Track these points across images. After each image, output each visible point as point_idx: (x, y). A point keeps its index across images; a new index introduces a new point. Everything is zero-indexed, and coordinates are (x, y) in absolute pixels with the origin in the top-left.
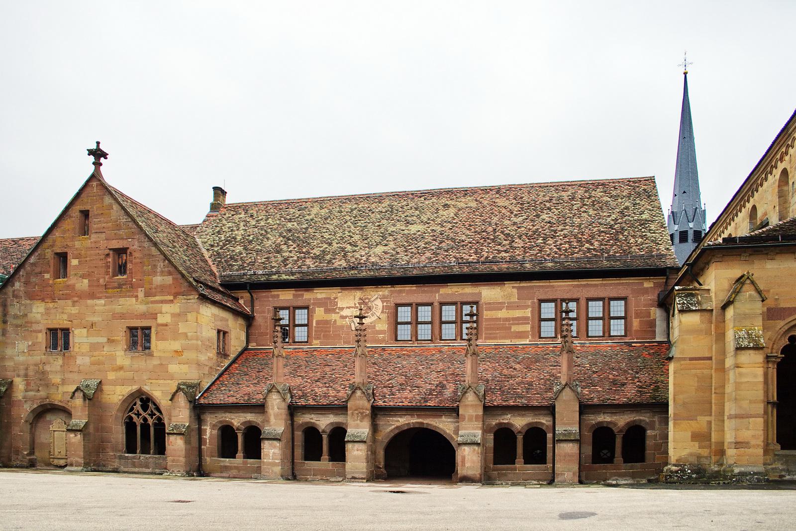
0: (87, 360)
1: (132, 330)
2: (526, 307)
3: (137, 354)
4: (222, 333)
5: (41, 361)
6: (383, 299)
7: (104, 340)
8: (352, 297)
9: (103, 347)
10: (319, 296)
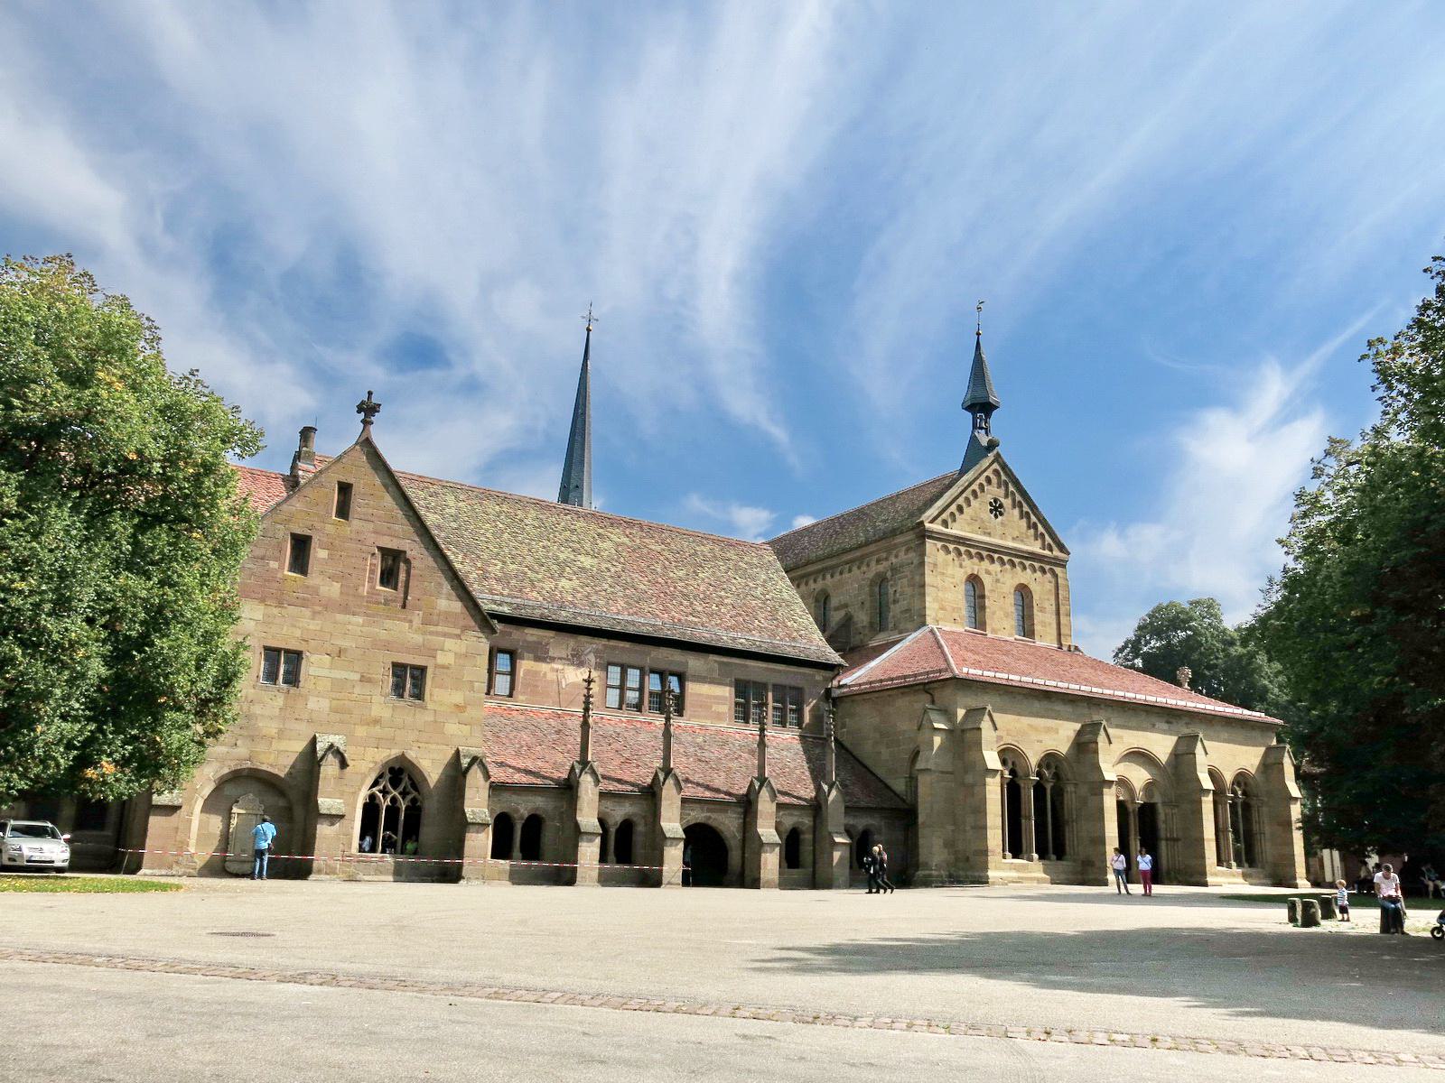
1: (399, 669)
6: (596, 652)
8: (564, 647)
9: (354, 687)
10: (530, 639)
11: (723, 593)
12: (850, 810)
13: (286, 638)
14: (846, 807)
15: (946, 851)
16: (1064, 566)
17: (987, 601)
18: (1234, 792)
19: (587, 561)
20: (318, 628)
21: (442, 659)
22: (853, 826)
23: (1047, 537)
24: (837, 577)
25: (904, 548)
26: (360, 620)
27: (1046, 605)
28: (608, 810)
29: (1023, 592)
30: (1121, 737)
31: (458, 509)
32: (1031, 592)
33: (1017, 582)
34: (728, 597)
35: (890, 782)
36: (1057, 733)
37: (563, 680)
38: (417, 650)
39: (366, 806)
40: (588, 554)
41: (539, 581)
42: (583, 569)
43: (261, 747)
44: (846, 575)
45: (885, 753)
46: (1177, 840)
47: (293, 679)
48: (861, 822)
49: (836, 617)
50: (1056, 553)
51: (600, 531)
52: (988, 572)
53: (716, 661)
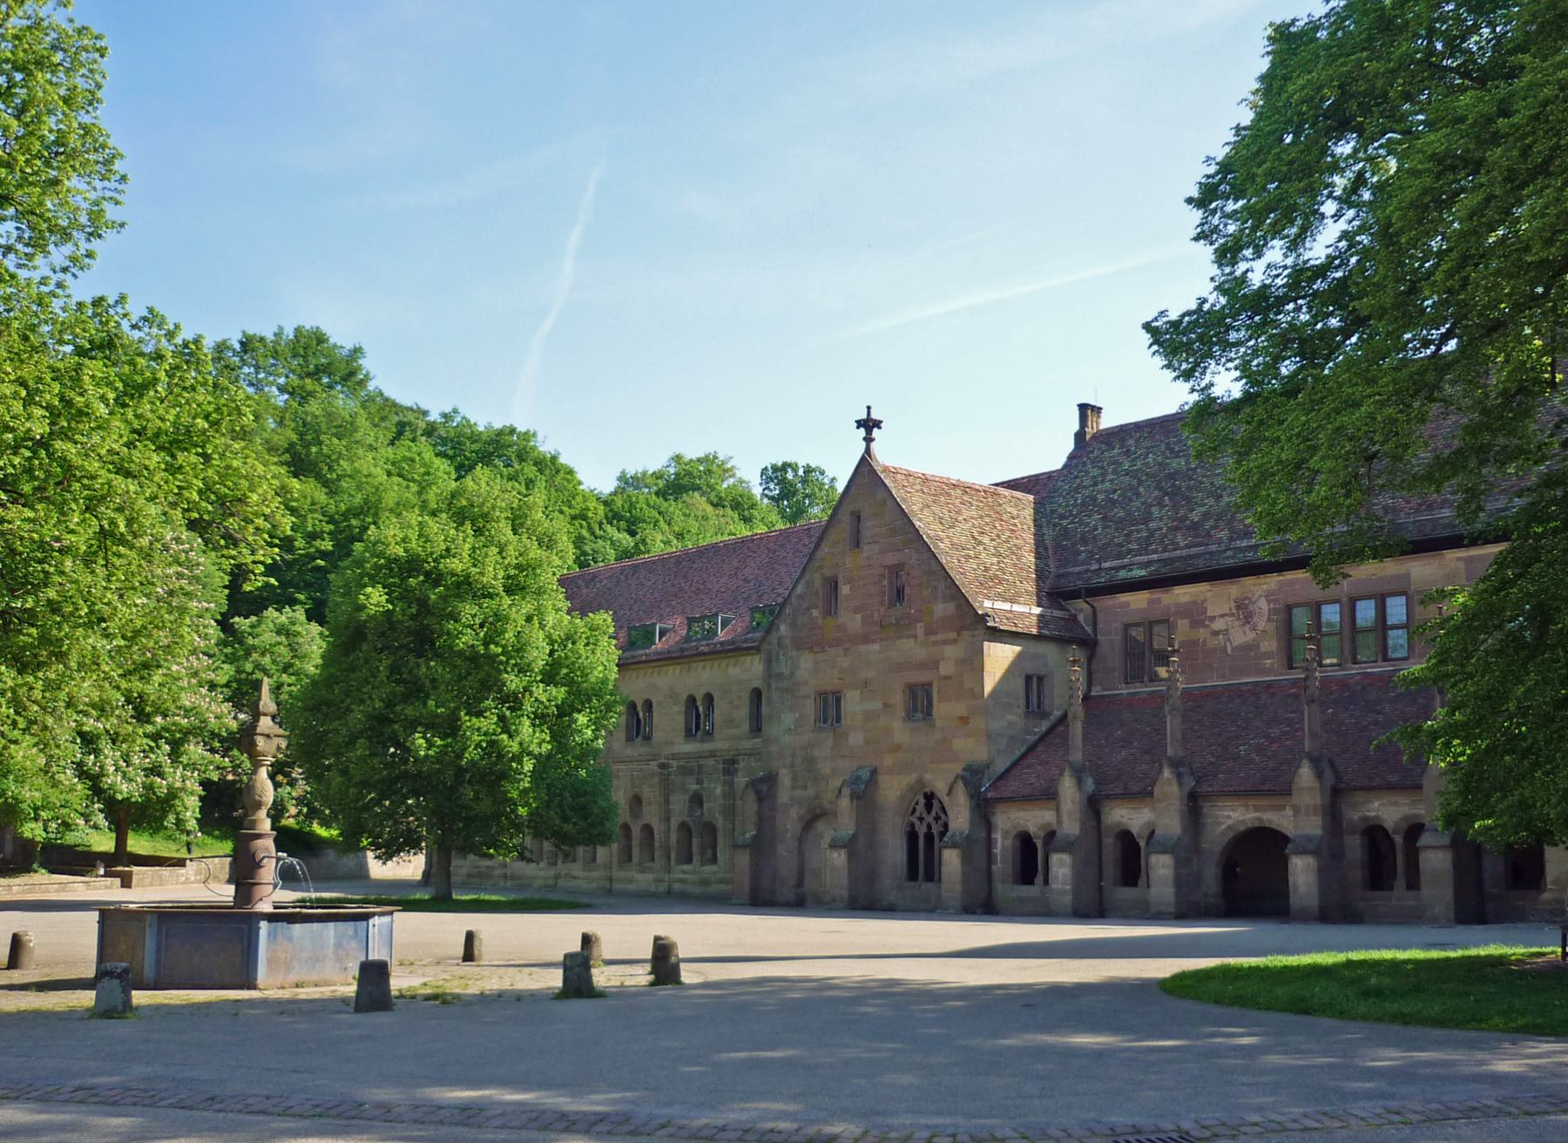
4: (1035, 679)
6: (1269, 596)
7: (878, 705)
10: (1183, 599)
13: (829, 680)
21: (946, 669)
26: (876, 647)
28: (1125, 820)
37: (1228, 644)
38: (923, 666)
53: (1459, 559)
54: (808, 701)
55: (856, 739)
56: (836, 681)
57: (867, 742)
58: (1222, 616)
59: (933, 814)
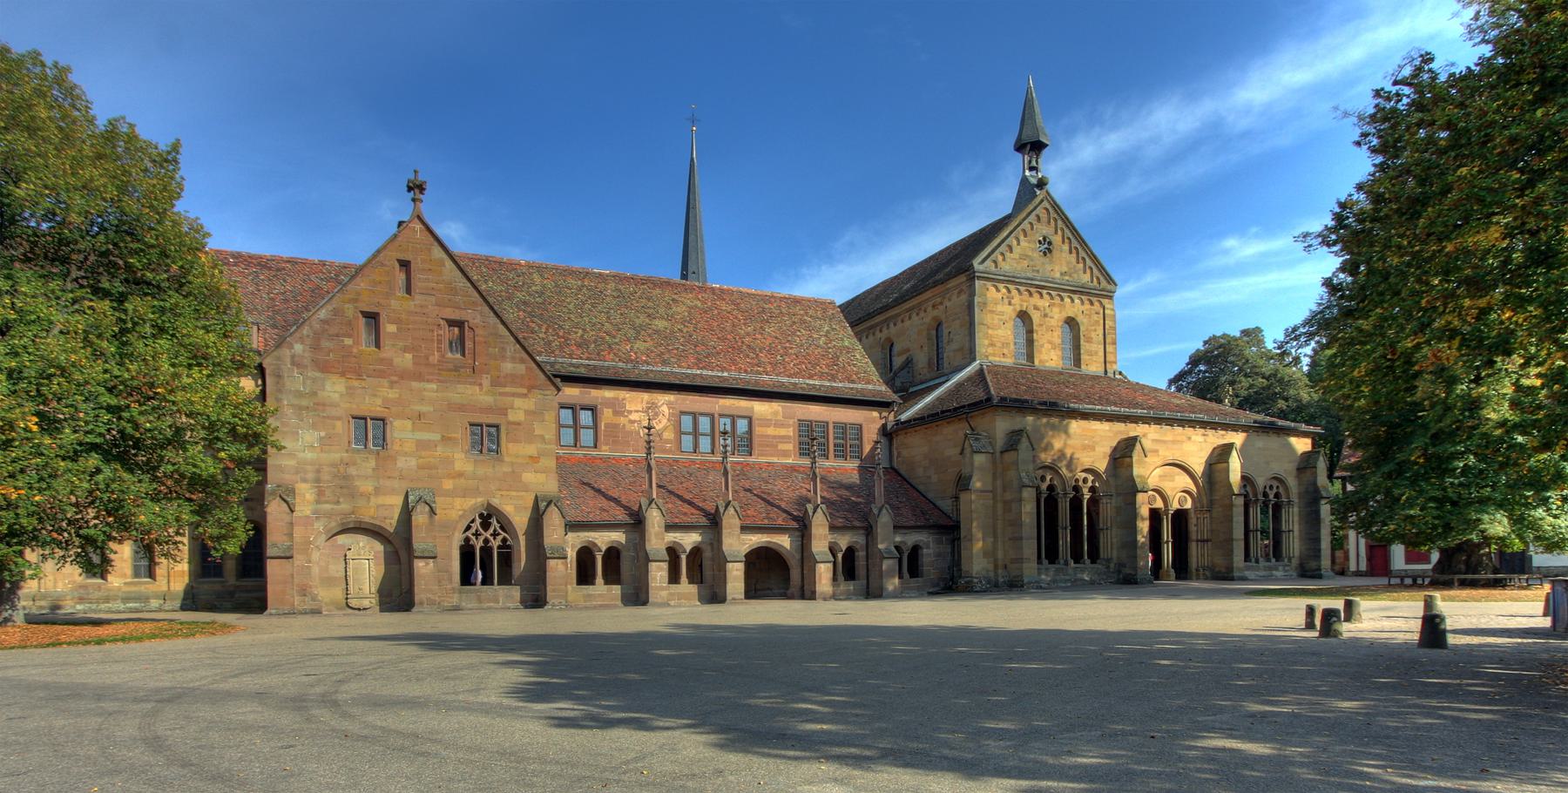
0: (413, 462)
2: (789, 426)
3: (481, 457)
5: (342, 460)
6: (669, 404)
7: (437, 437)
11: (787, 345)
12: (897, 528)
13: (371, 405)
14: (895, 527)
15: (986, 560)
16: (1110, 298)
17: (1035, 335)
18: (1265, 495)
19: (660, 324)
20: (397, 396)
21: (512, 417)
22: (904, 543)
23: (1095, 271)
24: (900, 325)
25: (956, 292)
26: (434, 386)
27: (1093, 335)
29: (1071, 323)
30: (1157, 451)
31: (544, 286)
32: (1078, 324)
33: (1064, 315)
34: (791, 348)
35: (939, 503)
36: (1094, 450)
38: (488, 410)
39: (462, 547)
40: (663, 318)
41: (616, 343)
42: (657, 332)
43: (361, 503)
44: (907, 323)
45: (935, 478)
46: (1207, 541)
47: (382, 441)
48: (912, 539)
49: (898, 361)
50: (1104, 283)
51: (675, 297)
52: (1036, 308)
54: (339, 424)
55: (407, 463)
56: (378, 409)
57: (420, 467)
58: (637, 411)
59: (491, 531)
